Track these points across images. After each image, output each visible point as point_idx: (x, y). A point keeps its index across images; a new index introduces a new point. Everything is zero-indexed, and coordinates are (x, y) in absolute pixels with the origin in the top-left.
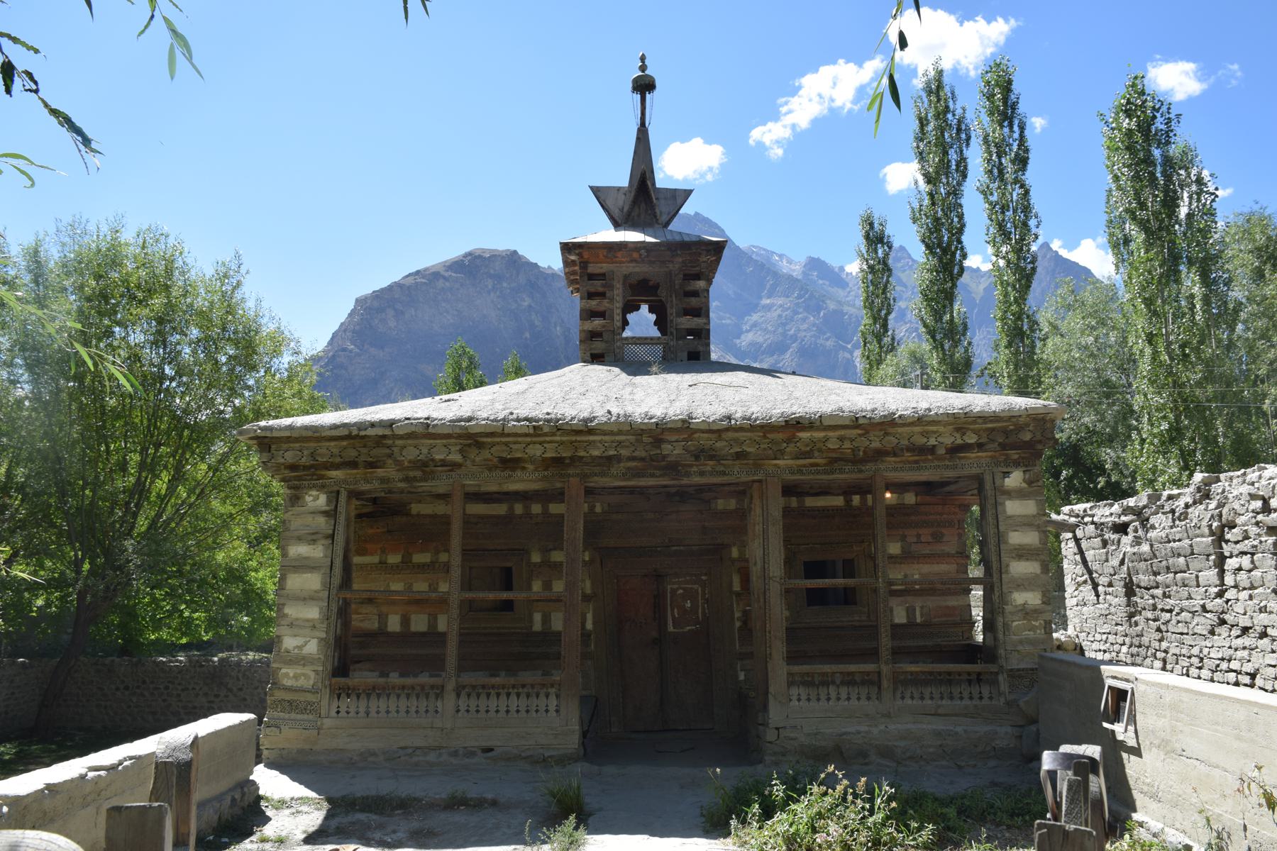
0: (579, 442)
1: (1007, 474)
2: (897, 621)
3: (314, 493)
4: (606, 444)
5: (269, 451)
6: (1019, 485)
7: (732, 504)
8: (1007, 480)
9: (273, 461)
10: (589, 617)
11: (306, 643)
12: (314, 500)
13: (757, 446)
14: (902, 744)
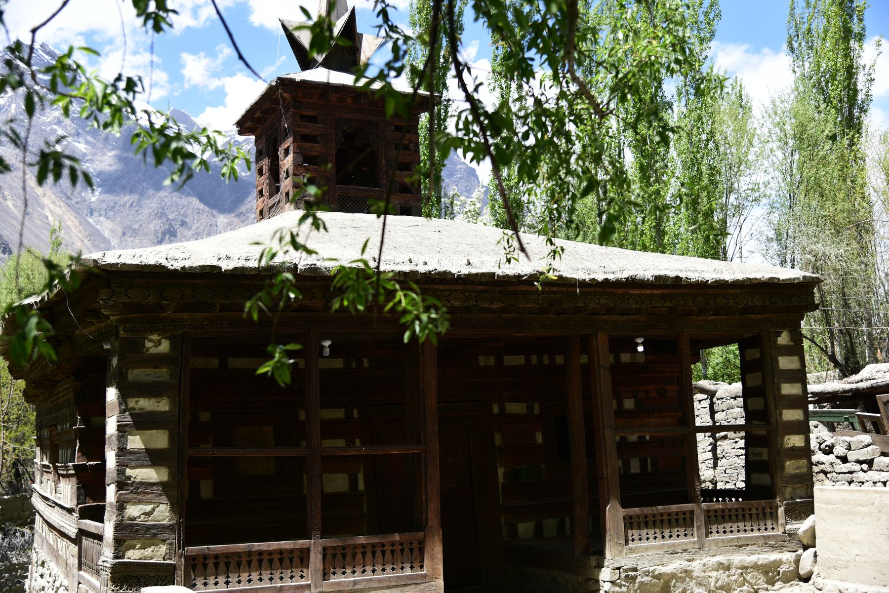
0: (441, 291)
1: (779, 334)
2: (633, 471)
3: (155, 337)
4: (466, 294)
5: (109, 288)
6: (787, 343)
7: (492, 361)
8: (779, 339)
9: (114, 299)
10: (361, 477)
11: (153, 510)
12: (155, 346)
13: (598, 302)
14: (714, 574)
